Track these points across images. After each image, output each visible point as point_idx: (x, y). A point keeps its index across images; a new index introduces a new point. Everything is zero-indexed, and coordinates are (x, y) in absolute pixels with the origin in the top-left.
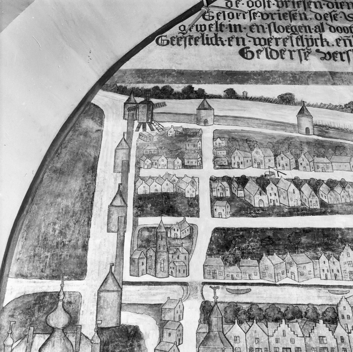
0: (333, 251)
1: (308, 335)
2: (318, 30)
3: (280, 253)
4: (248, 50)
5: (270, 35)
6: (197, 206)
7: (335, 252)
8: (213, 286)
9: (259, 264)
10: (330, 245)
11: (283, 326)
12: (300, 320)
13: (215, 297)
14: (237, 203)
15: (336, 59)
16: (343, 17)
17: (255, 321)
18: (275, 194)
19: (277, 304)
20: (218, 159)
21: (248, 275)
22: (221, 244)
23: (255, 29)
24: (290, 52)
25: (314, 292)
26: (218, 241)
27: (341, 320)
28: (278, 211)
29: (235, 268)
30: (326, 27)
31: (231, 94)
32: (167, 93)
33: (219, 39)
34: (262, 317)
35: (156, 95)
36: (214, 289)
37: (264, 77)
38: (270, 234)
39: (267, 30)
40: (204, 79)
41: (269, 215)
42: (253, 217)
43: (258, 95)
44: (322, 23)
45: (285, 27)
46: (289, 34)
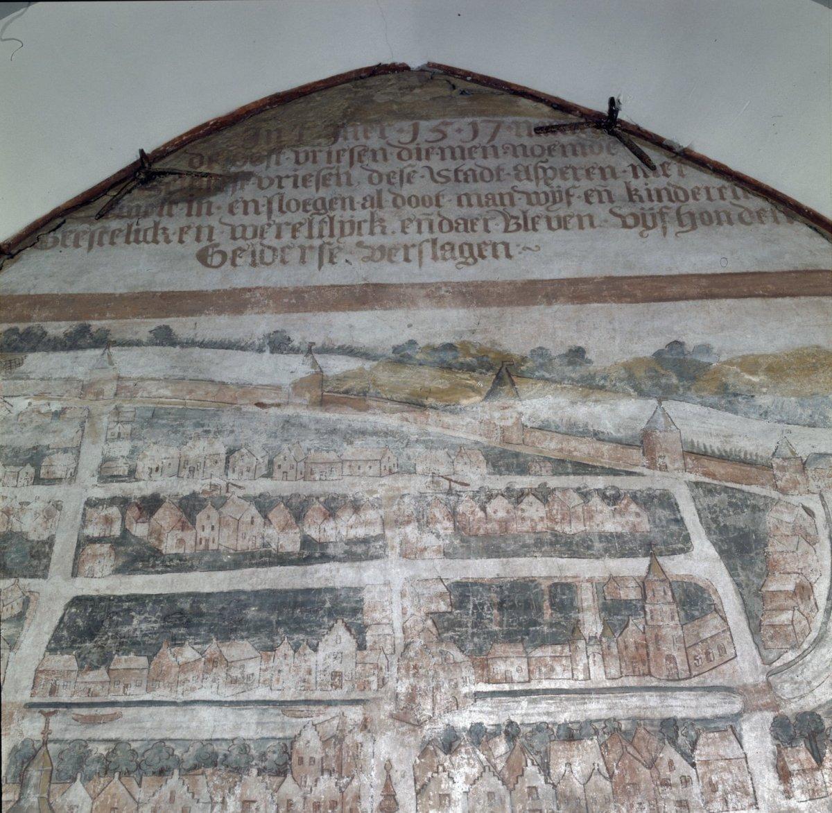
0: (307, 633)
1: (220, 799)
2: (368, 204)
3: (198, 641)
5: (269, 218)
6: (48, 556)
7: (312, 635)
8: (46, 710)
11: (174, 781)
12: (209, 771)
13: (46, 731)
15: (394, 259)
16: (428, 175)
17: (117, 775)
18: (213, 528)
19: (171, 740)
21: (122, 686)
22: (79, 627)
23: (239, 209)
24: (303, 248)
25: (250, 716)
27: (296, 768)
29: (101, 674)
30: (387, 198)
31: (165, 338)
32: (37, 342)
33: (160, 232)
34: (134, 767)
35: (9, 345)
36: (47, 715)
37: (235, 301)
38: (186, 605)
39: (264, 209)
41: (191, 569)
42: (158, 572)
45: (301, 201)
46: (307, 215)
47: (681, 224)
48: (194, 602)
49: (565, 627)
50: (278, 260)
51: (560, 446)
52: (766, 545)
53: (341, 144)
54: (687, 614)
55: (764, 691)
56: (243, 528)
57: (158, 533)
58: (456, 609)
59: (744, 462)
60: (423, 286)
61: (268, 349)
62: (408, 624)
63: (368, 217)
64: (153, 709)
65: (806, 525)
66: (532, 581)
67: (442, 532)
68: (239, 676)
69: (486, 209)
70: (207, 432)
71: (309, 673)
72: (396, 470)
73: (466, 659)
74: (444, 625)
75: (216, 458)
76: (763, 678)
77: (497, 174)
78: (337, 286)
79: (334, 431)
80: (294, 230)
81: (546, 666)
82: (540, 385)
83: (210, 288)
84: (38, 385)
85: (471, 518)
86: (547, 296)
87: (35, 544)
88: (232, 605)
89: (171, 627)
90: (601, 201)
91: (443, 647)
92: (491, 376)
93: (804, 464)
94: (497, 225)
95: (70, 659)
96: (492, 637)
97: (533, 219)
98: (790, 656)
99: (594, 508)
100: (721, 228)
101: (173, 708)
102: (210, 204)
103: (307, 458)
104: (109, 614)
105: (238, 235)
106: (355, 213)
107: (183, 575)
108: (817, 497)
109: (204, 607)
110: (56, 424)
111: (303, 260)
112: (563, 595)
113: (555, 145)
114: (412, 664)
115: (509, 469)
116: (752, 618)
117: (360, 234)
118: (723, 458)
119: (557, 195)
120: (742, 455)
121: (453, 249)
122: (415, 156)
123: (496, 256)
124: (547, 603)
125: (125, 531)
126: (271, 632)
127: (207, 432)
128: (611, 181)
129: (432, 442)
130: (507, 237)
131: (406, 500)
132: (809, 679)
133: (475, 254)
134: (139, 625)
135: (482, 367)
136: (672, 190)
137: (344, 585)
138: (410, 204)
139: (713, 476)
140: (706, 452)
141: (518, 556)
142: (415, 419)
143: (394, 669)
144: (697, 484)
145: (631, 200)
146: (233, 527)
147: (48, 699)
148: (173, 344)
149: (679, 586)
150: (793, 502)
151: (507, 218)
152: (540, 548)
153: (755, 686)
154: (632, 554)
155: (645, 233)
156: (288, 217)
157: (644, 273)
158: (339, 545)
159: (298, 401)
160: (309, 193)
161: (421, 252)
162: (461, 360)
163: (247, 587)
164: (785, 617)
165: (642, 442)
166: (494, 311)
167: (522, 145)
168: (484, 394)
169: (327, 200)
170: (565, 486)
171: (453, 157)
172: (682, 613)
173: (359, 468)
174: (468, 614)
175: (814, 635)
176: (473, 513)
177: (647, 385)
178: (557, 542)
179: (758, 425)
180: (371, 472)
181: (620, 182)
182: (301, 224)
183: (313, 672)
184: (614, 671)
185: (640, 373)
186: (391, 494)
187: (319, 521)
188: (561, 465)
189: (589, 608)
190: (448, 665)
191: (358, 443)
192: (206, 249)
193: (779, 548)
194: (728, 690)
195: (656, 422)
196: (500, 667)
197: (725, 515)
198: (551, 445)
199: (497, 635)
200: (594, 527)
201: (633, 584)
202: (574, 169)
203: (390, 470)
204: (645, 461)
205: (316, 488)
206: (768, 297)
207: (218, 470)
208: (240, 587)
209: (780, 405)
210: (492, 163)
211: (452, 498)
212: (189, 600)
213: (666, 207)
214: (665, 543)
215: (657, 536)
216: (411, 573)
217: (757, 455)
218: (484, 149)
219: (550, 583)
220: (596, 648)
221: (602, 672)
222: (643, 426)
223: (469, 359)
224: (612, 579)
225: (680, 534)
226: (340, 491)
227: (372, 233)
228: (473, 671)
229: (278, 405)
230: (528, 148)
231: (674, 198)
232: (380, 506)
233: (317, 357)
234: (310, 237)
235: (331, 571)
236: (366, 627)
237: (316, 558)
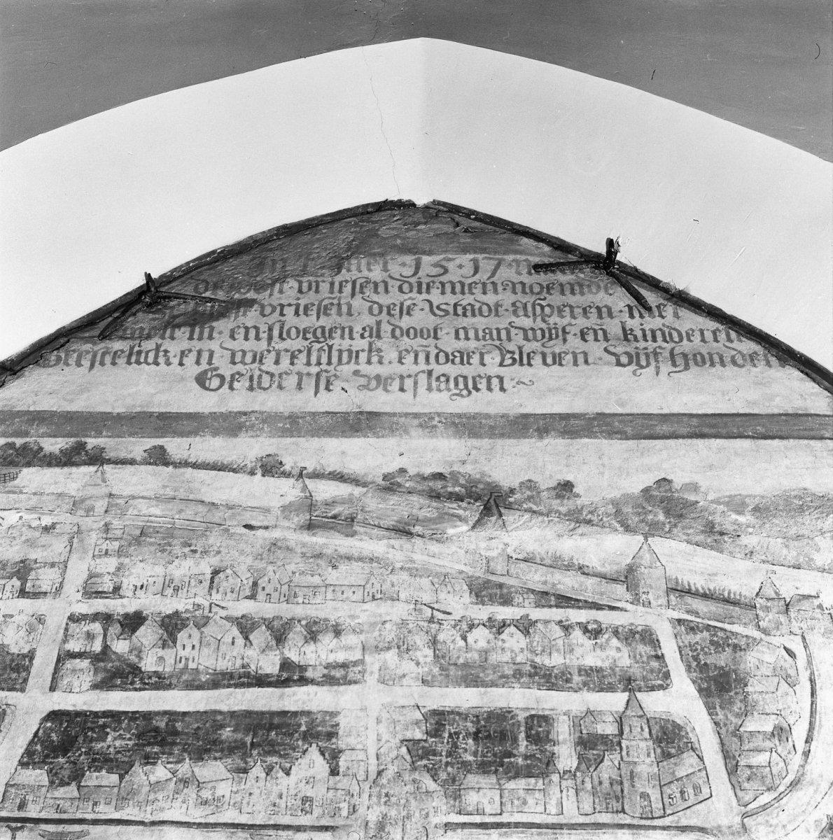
0: (281, 756)
2: (367, 334)
3: (171, 760)
4: (214, 373)
5: (269, 344)
6: (27, 669)
8: (14, 825)
9: (121, 782)
10: (279, 744)
14: (110, 665)
15: (389, 388)
18: (193, 647)
20: (93, 580)
21: (91, 803)
22: (53, 741)
23: (240, 335)
24: (300, 374)
26: (50, 737)
28: (190, 679)
29: (71, 791)
31: (159, 457)
32: (33, 457)
33: (161, 354)
36: (14, 830)
37: (231, 424)
39: (264, 336)
40: (109, 429)
41: (169, 687)
42: (136, 690)
43: (211, 458)
44: (380, 321)
45: (301, 329)
47: (674, 365)
48: (170, 721)
49: (540, 760)
50: (275, 386)
51: (544, 579)
52: (746, 685)
53: (344, 275)
54: (663, 752)
55: (739, 832)
56: (223, 648)
57: (138, 651)
58: (432, 737)
59: (727, 601)
60: (416, 415)
61: (259, 472)
62: (382, 750)
63: (366, 348)
64: (119, 828)
65: (787, 665)
66: (509, 712)
67: (421, 660)
68: (210, 797)
69: (483, 343)
70: (194, 551)
71: (281, 797)
72: (379, 596)
73: (439, 788)
74: (418, 752)
75: (201, 577)
76: (738, 819)
77: (495, 310)
78: (329, 413)
79: (319, 556)
80: (293, 357)
81: (518, 799)
82: (527, 516)
83: (207, 411)
84: (30, 499)
85: (452, 647)
86: (538, 430)
87: (15, 657)
88: (207, 725)
89: (144, 745)
90: (596, 340)
91: (416, 775)
92: (479, 506)
93: (787, 605)
94: (493, 359)
95: (41, 774)
96: (465, 765)
97: (528, 355)
98: (766, 798)
99: (575, 641)
100: (714, 370)
101: (141, 827)
102: (212, 329)
103: (291, 581)
104: (84, 730)
105: (238, 359)
106: (353, 342)
107: (160, 693)
108: (799, 639)
109: (179, 726)
110: (45, 539)
111: (299, 387)
112: (539, 727)
113: (553, 284)
114: (384, 791)
115: (492, 599)
116: (729, 758)
117: (357, 363)
118: (706, 596)
119: (553, 331)
120: (726, 595)
121: (448, 380)
122: (415, 289)
123: (489, 389)
124: (522, 735)
125: (106, 648)
126: (245, 754)
127: (194, 551)
128: (607, 320)
129: (417, 570)
130: (502, 371)
131: (388, 626)
132: (785, 823)
133: (470, 386)
134: (113, 742)
135: (470, 497)
136: (667, 331)
137: (320, 709)
138: (408, 336)
139: (697, 614)
140: (690, 589)
141: (497, 686)
142: (401, 546)
143: (365, 796)
144: (679, 621)
145: (626, 339)
146: (213, 647)
147: (17, 814)
148: (166, 464)
149: (656, 723)
150: (774, 642)
151: (503, 352)
152: (519, 679)
153: (729, 827)
154: (611, 688)
155: (638, 372)
156: (288, 344)
157: (635, 411)
158: (319, 668)
159: (286, 524)
160: (309, 321)
161: (416, 383)
162: (450, 489)
163: (224, 708)
164: (760, 759)
165: (626, 577)
166: (485, 443)
167: (521, 283)
168: (471, 523)
169: (327, 329)
170: (548, 618)
171: (453, 292)
172: (659, 751)
173: (343, 593)
174: (443, 743)
175: (791, 777)
176: (453, 641)
177: (634, 520)
178: (536, 674)
179: (743, 565)
180: (354, 598)
181: (616, 321)
182: (300, 351)
183: (284, 797)
184: (587, 807)
185: (628, 510)
186: (372, 620)
187: (300, 645)
188: (544, 597)
189: (565, 742)
190: (421, 794)
191: (343, 567)
192: (205, 372)
193: (759, 688)
194: (702, 830)
195: (641, 558)
196: (472, 799)
197: (706, 654)
198: (536, 578)
199: (471, 765)
200: (573, 661)
201: (611, 719)
202: (571, 307)
203: (373, 596)
204: (628, 596)
205: (299, 611)
206: (757, 438)
207: (202, 590)
208: (218, 708)
209: (765, 545)
210: (491, 298)
211: (433, 626)
212: (165, 719)
213: (660, 347)
214: (644, 678)
215: (636, 671)
216: (389, 700)
217: (740, 595)
218: (484, 285)
219: (527, 714)
220: (570, 783)
221: (576, 806)
222: (629, 561)
223: (457, 489)
224: (589, 712)
225: (660, 671)
226: (322, 615)
227: (369, 362)
228: (445, 801)
229: (266, 528)
230: (527, 286)
231: (668, 339)
232: (362, 631)
233: (307, 481)
234: (308, 364)
235: (309, 695)
236: (340, 752)
237: (294, 681)
